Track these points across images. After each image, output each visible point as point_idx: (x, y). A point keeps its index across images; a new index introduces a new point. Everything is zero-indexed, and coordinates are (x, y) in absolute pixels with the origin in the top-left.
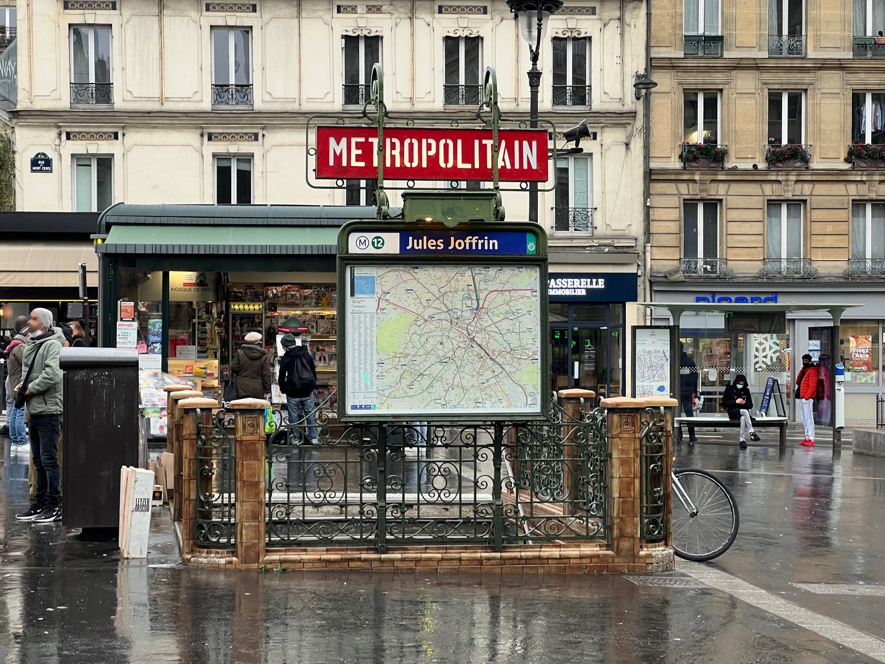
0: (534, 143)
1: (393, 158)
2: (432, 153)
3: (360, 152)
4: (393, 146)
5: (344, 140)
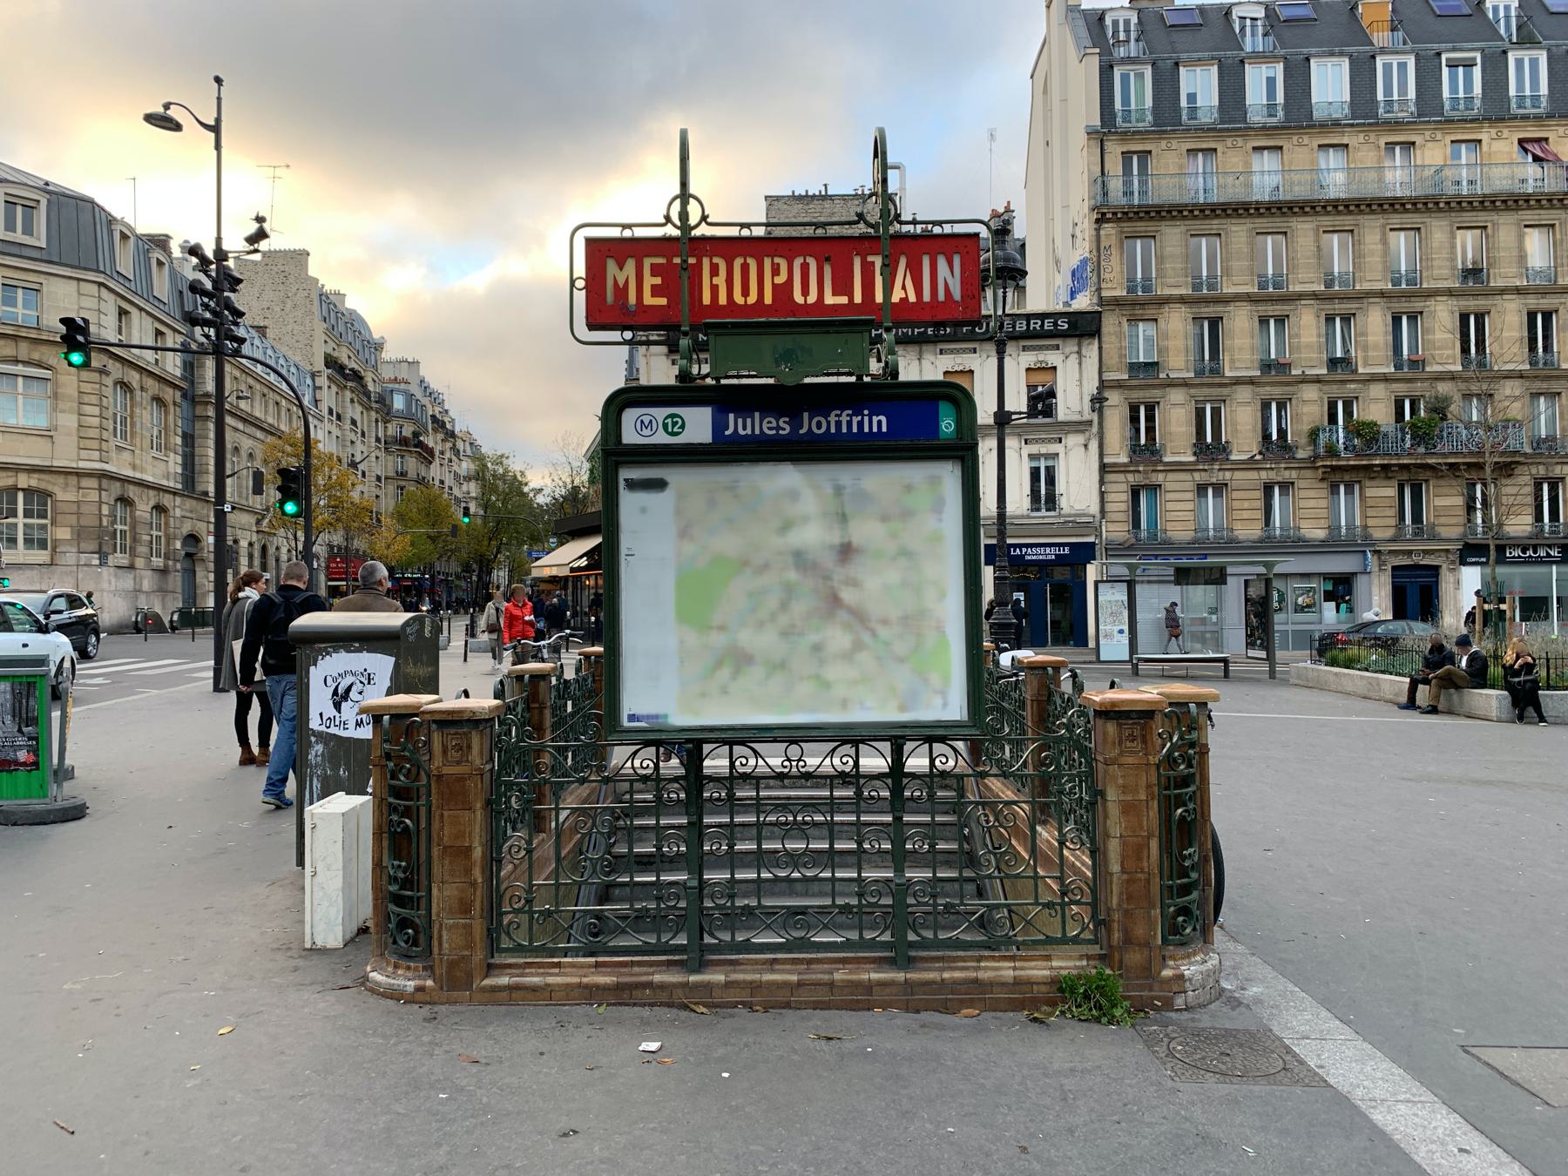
0: (957, 260)
1: (714, 289)
2: (781, 279)
3: (658, 281)
4: (714, 271)
5: (630, 265)
